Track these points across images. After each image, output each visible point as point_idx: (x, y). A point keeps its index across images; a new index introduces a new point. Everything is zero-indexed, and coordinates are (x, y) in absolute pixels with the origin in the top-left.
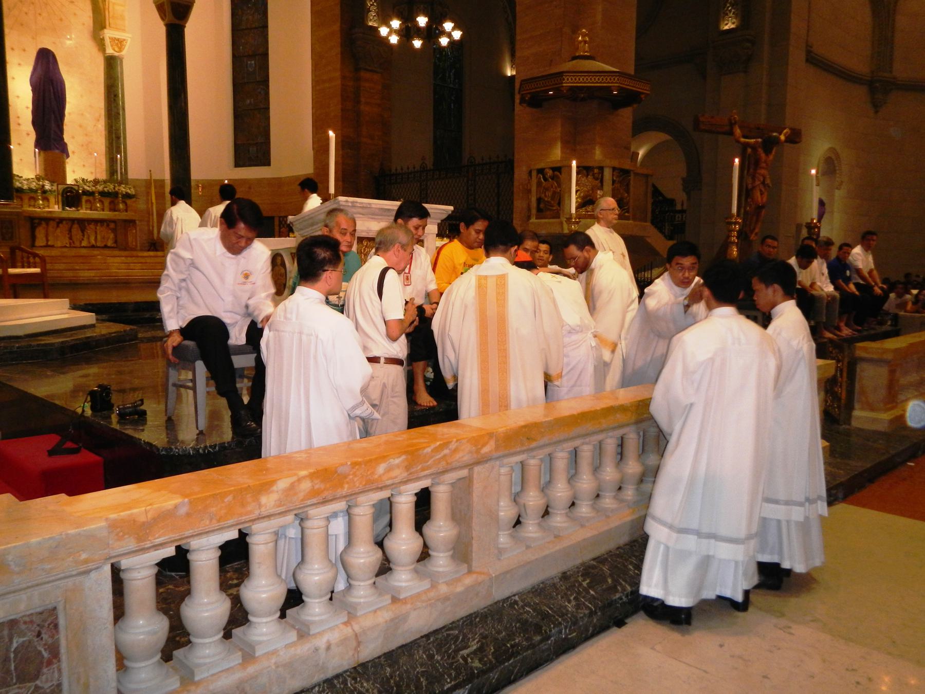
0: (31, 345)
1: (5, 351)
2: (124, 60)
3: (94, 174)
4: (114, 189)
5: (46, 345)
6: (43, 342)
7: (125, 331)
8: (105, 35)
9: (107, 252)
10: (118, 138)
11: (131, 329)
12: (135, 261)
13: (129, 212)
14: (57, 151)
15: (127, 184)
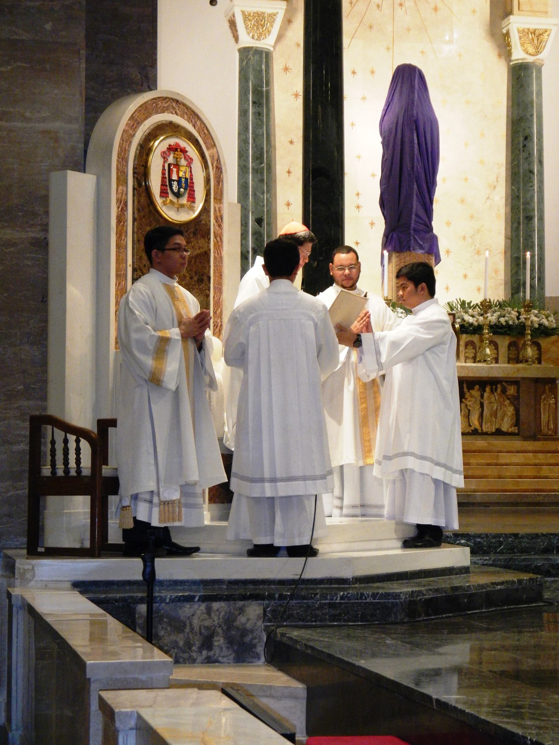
0: (362, 594)
1: (324, 601)
2: (543, 69)
3: (482, 291)
4: (518, 318)
5: (387, 595)
6: (381, 591)
7: (520, 581)
8: (510, 27)
9: (498, 443)
10: (529, 219)
11: (530, 579)
12: (552, 461)
13: (543, 363)
14: (420, 252)
15: (542, 308)
